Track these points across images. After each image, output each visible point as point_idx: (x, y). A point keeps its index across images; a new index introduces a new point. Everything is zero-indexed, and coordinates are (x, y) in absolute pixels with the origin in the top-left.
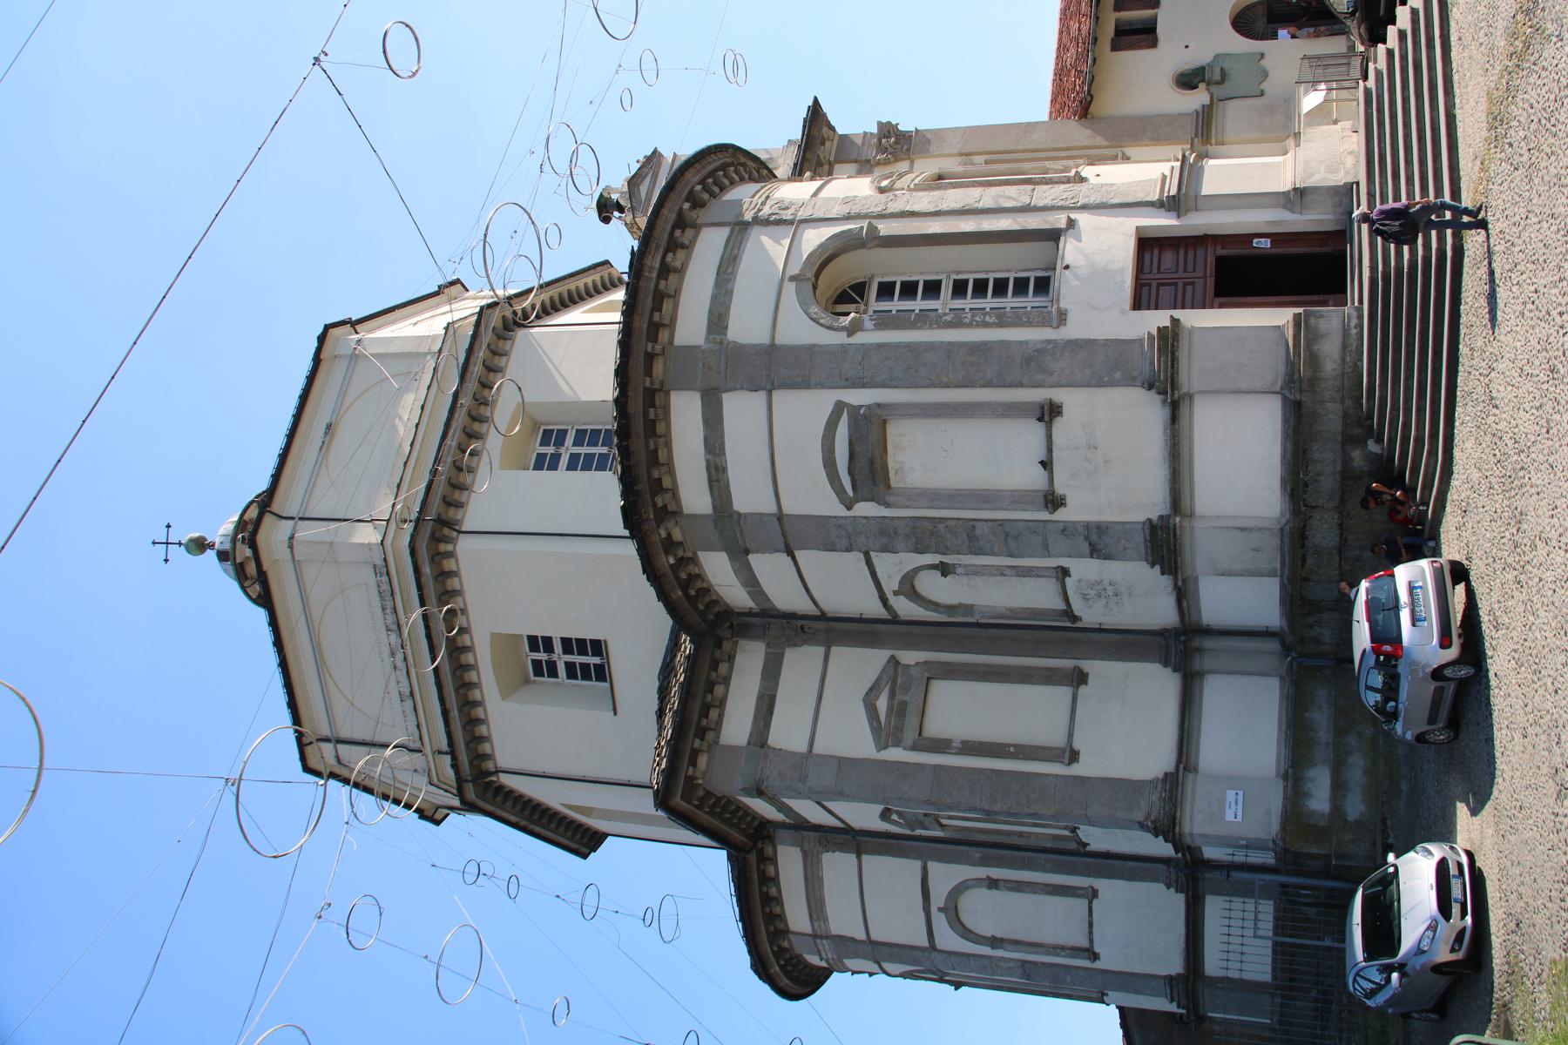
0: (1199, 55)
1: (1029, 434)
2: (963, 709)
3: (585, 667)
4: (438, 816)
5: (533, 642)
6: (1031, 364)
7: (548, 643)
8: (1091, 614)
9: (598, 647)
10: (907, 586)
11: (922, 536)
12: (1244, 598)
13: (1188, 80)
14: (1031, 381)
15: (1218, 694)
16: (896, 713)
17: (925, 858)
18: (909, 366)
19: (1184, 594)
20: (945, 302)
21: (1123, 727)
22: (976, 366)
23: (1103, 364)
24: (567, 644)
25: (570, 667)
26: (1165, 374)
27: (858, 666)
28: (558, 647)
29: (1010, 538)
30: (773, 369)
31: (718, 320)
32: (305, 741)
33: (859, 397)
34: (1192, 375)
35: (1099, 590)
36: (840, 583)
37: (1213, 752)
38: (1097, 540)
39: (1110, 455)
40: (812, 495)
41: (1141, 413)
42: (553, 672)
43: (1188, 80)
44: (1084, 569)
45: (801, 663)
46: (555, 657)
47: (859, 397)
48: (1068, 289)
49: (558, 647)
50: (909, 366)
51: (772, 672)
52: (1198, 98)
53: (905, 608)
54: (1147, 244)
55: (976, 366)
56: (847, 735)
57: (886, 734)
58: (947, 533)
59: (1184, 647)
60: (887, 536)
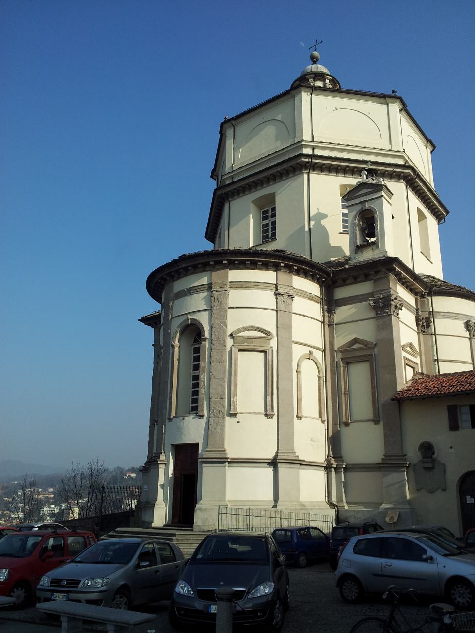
3: (267, 231)
4: (214, 177)
5: (273, 209)
7: (273, 215)
9: (274, 235)
24: (274, 223)
25: (267, 225)
28: (272, 220)
32: (233, 122)
42: (265, 218)
46: (270, 218)
49: (272, 220)
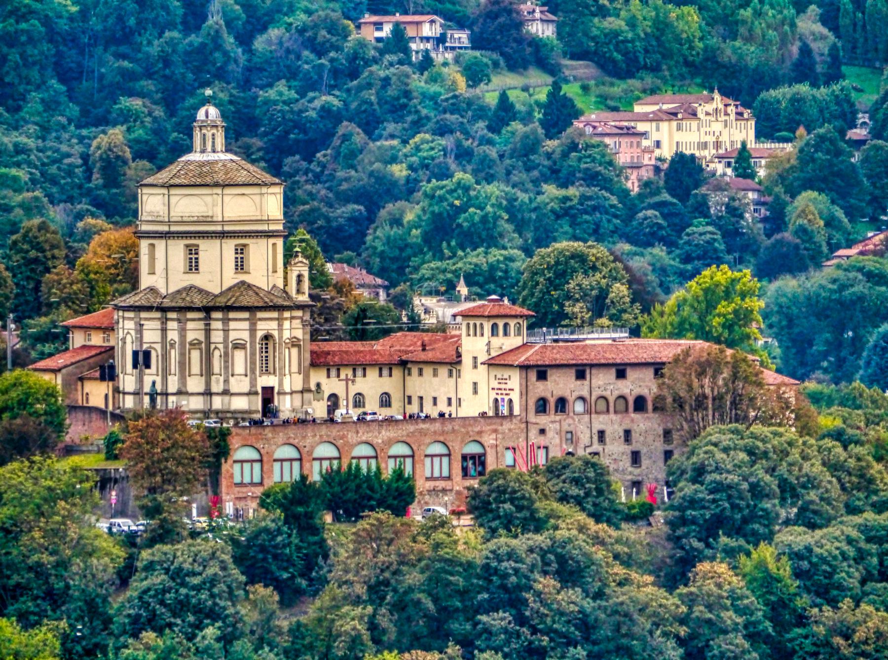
0: (324, 387)
1: (243, 372)
2: (195, 355)
6: (253, 371)
8: (213, 378)
10: (216, 348)
11: (226, 354)
12: (218, 403)
13: (318, 385)
14: (251, 372)
15: (200, 399)
16: (195, 344)
17: (162, 342)
18: (253, 354)
19: (218, 394)
20: (264, 354)
21: (195, 384)
22: (253, 363)
23: (253, 383)
26: (252, 393)
27: (201, 336)
29: (226, 368)
30: (253, 331)
31: (260, 319)
33: (248, 345)
34: (253, 397)
35: (218, 381)
36: (217, 337)
37: (193, 399)
38: (226, 381)
39: (240, 384)
40: (233, 335)
41: (246, 389)
43: (318, 385)
44: (222, 379)
45: (201, 325)
47: (248, 345)
48: (265, 377)
50: (253, 354)
51: (200, 319)
52: (313, 388)
53: (213, 346)
54: (272, 388)
55: (253, 363)
56: (190, 336)
57: (191, 344)
58: (227, 357)
59: (208, 393)
60: (226, 347)
